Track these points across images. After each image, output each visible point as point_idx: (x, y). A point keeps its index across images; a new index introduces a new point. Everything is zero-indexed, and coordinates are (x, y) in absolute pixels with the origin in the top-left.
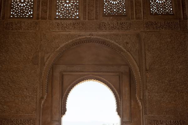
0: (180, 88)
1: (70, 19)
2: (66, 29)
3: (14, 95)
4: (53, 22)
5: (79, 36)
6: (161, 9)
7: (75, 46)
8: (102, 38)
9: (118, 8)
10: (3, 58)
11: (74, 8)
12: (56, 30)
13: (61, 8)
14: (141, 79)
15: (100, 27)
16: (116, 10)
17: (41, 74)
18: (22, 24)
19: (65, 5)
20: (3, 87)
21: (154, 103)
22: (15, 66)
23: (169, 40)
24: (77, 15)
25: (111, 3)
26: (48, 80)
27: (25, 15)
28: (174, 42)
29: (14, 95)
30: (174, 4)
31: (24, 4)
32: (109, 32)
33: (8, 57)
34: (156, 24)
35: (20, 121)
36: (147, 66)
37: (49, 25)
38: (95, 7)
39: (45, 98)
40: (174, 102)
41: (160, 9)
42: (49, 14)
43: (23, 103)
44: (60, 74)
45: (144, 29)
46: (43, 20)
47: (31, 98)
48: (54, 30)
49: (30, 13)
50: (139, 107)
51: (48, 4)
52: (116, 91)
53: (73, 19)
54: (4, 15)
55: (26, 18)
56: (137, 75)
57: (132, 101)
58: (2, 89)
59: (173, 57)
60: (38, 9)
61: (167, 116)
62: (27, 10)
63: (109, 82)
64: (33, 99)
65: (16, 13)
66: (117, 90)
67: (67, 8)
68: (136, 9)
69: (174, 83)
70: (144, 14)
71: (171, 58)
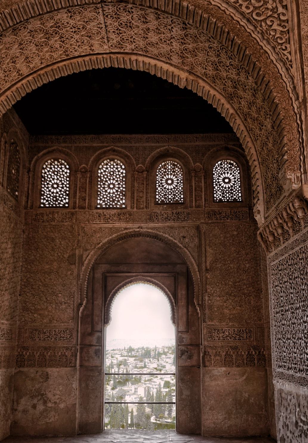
0: (247, 290)
1: (113, 208)
2: (109, 220)
3: (46, 302)
4: (93, 212)
5: (126, 229)
6: (228, 195)
7: (120, 242)
8: (154, 231)
9: (174, 195)
10: (33, 257)
11: (119, 195)
12: (97, 222)
13: (104, 195)
14: (200, 281)
15: (151, 218)
16: (172, 197)
17: (78, 275)
18: (55, 215)
19: (108, 191)
20: (33, 292)
21: (215, 309)
22: (48, 267)
23: (235, 233)
24: (123, 204)
25: (165, 188)
26: (87, 283)
27: (59, 203)
28: (241, 235)
29: (46, 302)
30: (243, 188)
31: (58, 190)
32: (162, 224)
33: (38, 255)
34: (220, 213)
35: (54, 333)
36: (208, 264)
37: (88, 216)
38: (145, 193)
39: (84, 304)
40: (239, 308)
41: (226, 195)
42: (88, 202)
43: (57, 311)
44: (103, 275)
45: (205, 220)
46: (80, 210)
47: (66, 305)
48: (94, 222)
49: (64, 201)
50: (198, 313)
51: (87, 189)
52: (170, 295)
53: (117, 208)
54: (33, 203)
55: (60, 207)
56: (196, 276)
57: (190, 307)
58: (31, 294)
59: (240, 253)
60: (75, 196)
61: (231, 324)
62: (61, 198)
63: (163, 284)
64: (69, 306)
65: (47, 201)
66: (172, 294)
67: (111, 195)
68: (195, 195)
69: (240, 285)
70: (205, 201)
71: (237, 254)
